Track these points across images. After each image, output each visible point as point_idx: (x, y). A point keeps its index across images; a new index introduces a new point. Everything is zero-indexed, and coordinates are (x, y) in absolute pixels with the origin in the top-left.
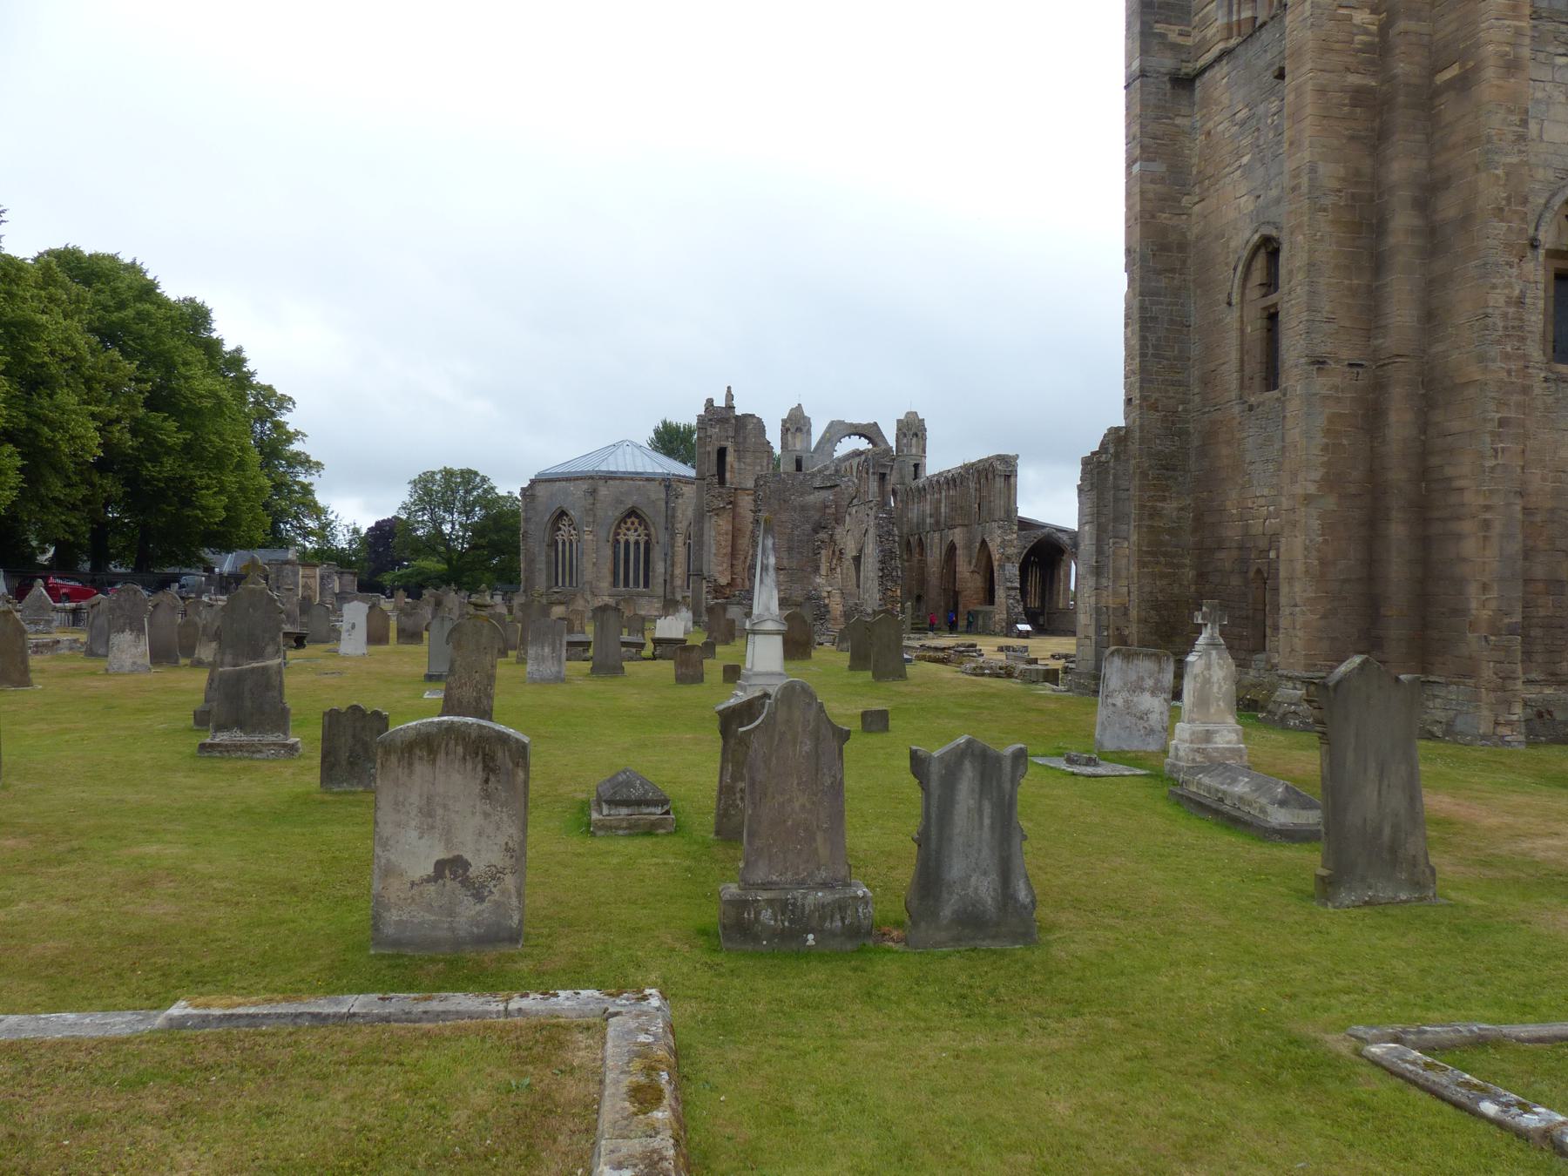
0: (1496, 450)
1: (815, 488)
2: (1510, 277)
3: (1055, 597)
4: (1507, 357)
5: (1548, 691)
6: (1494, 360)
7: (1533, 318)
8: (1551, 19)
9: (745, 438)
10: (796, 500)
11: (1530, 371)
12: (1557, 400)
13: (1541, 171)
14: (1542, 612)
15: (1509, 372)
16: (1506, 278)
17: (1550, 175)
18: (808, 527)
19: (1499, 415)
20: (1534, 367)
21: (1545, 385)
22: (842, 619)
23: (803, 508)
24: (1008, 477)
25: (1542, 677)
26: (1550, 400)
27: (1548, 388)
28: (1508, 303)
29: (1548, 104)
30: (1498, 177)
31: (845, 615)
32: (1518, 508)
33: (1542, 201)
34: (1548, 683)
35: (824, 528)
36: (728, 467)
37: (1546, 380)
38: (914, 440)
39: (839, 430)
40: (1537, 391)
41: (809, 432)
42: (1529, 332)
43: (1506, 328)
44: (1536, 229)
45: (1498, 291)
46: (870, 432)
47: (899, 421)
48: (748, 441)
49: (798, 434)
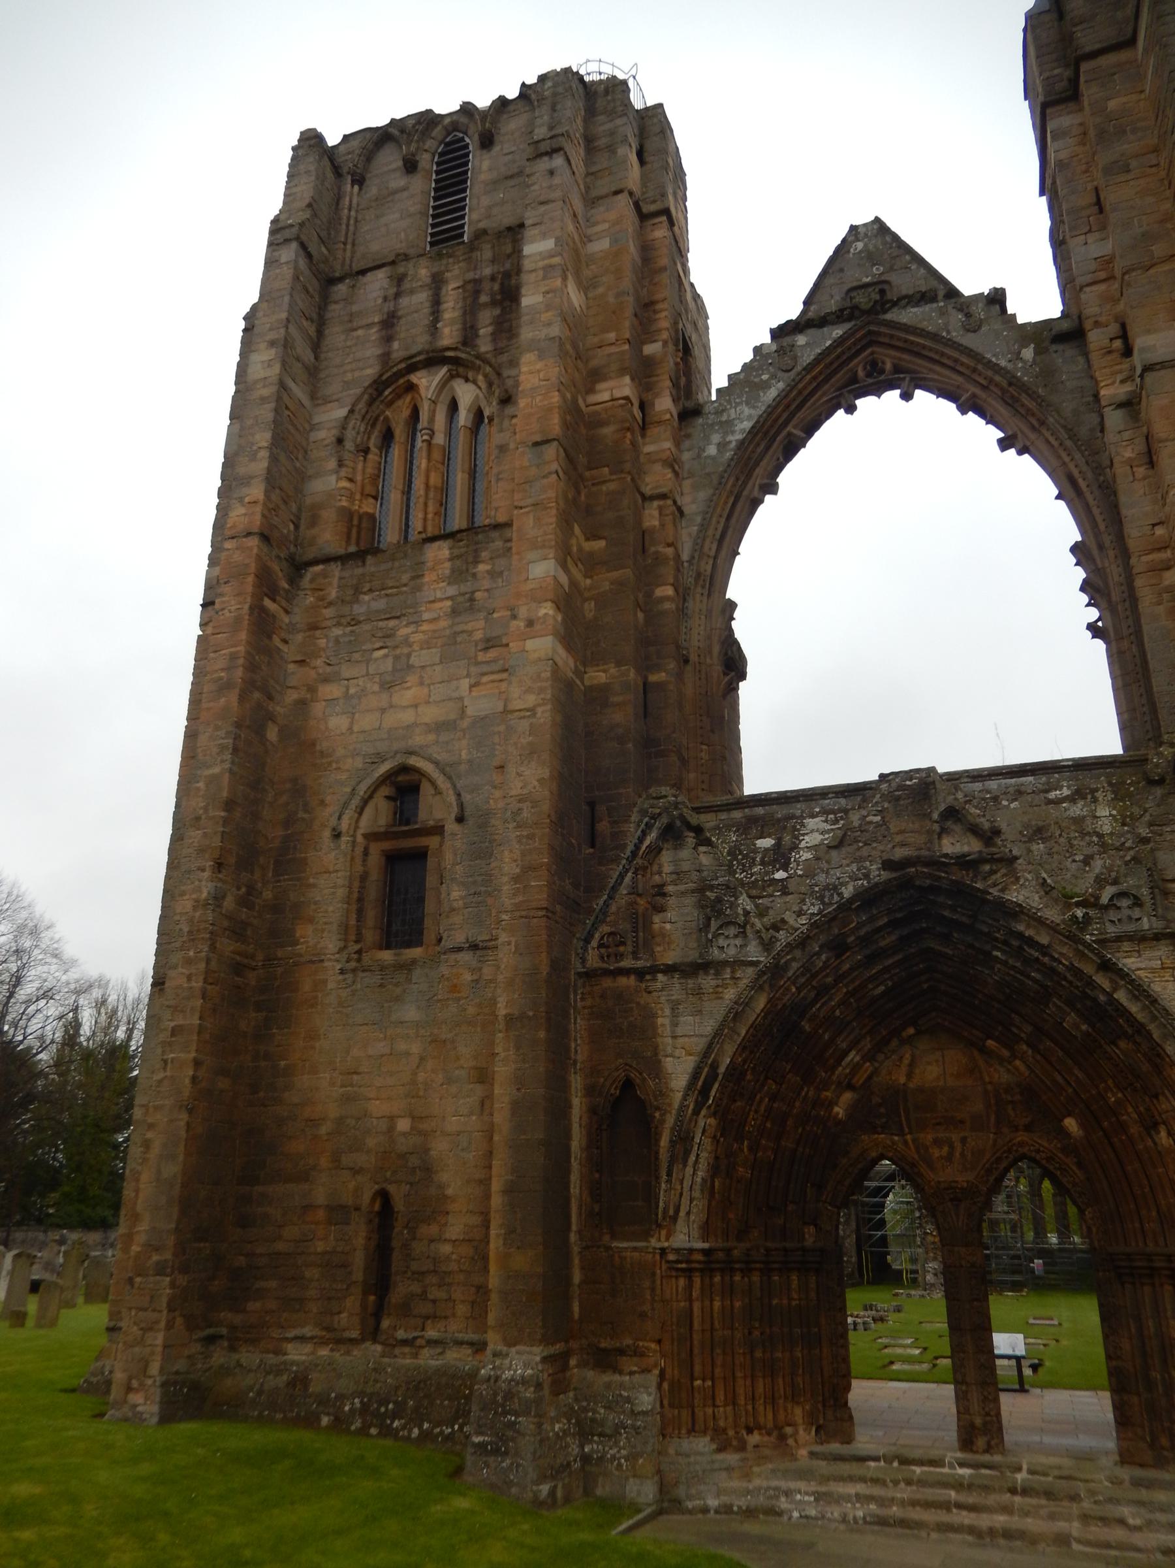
0: (165, 1062)
2: (200, 881)
4: (188, 962)
5: (324, 1352)
6: (175, 967)
7: (331, 909)
8: (369, 620)
11: (326, 964)
12: (354, 993)
13: (350, 760)
14: (320, 1246)
15: (189, 978)
16: (197, 883)
17: (359, 763)
19: (172, 1024)
20: (330, 960)
21: (341, 977)
25: (317, 1332)
26: (344, 994)
27: (345, 980)
28: (195, 908)
29: (360, 698)
30: (198, 789)
32: (182, 1123)
33: (348, 790)
34: (323, 1342)
37: (342, 971)
40: (331, 985)
42: (326, 923)
43: (190, 932)
44: (339, 818)
45: (187, 897)
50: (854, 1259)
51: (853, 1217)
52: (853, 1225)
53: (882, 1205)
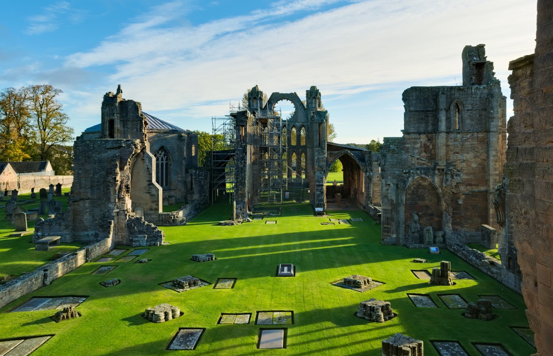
1: (107, 149)
3: (360, 185)
9: (127, 114)
10: (96, 156)
18: (103, 173)
22: (126, 229)
23: (100, 161)
24: (320, 124)
31: (128, 224)
35: (111, 174)
36: (116, 131)
38: (314, 100)
39: (276, 97)
41: (261, 99)
46: (293, 97)
47: (307, 91)
48: (129, 115)
49: (255, 100)
50: (207, 195)
51: (209, 176)
52: (208, 180)
53: (224, 170)
